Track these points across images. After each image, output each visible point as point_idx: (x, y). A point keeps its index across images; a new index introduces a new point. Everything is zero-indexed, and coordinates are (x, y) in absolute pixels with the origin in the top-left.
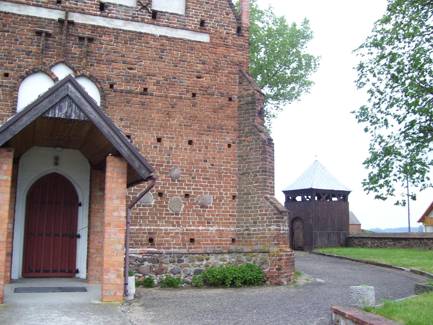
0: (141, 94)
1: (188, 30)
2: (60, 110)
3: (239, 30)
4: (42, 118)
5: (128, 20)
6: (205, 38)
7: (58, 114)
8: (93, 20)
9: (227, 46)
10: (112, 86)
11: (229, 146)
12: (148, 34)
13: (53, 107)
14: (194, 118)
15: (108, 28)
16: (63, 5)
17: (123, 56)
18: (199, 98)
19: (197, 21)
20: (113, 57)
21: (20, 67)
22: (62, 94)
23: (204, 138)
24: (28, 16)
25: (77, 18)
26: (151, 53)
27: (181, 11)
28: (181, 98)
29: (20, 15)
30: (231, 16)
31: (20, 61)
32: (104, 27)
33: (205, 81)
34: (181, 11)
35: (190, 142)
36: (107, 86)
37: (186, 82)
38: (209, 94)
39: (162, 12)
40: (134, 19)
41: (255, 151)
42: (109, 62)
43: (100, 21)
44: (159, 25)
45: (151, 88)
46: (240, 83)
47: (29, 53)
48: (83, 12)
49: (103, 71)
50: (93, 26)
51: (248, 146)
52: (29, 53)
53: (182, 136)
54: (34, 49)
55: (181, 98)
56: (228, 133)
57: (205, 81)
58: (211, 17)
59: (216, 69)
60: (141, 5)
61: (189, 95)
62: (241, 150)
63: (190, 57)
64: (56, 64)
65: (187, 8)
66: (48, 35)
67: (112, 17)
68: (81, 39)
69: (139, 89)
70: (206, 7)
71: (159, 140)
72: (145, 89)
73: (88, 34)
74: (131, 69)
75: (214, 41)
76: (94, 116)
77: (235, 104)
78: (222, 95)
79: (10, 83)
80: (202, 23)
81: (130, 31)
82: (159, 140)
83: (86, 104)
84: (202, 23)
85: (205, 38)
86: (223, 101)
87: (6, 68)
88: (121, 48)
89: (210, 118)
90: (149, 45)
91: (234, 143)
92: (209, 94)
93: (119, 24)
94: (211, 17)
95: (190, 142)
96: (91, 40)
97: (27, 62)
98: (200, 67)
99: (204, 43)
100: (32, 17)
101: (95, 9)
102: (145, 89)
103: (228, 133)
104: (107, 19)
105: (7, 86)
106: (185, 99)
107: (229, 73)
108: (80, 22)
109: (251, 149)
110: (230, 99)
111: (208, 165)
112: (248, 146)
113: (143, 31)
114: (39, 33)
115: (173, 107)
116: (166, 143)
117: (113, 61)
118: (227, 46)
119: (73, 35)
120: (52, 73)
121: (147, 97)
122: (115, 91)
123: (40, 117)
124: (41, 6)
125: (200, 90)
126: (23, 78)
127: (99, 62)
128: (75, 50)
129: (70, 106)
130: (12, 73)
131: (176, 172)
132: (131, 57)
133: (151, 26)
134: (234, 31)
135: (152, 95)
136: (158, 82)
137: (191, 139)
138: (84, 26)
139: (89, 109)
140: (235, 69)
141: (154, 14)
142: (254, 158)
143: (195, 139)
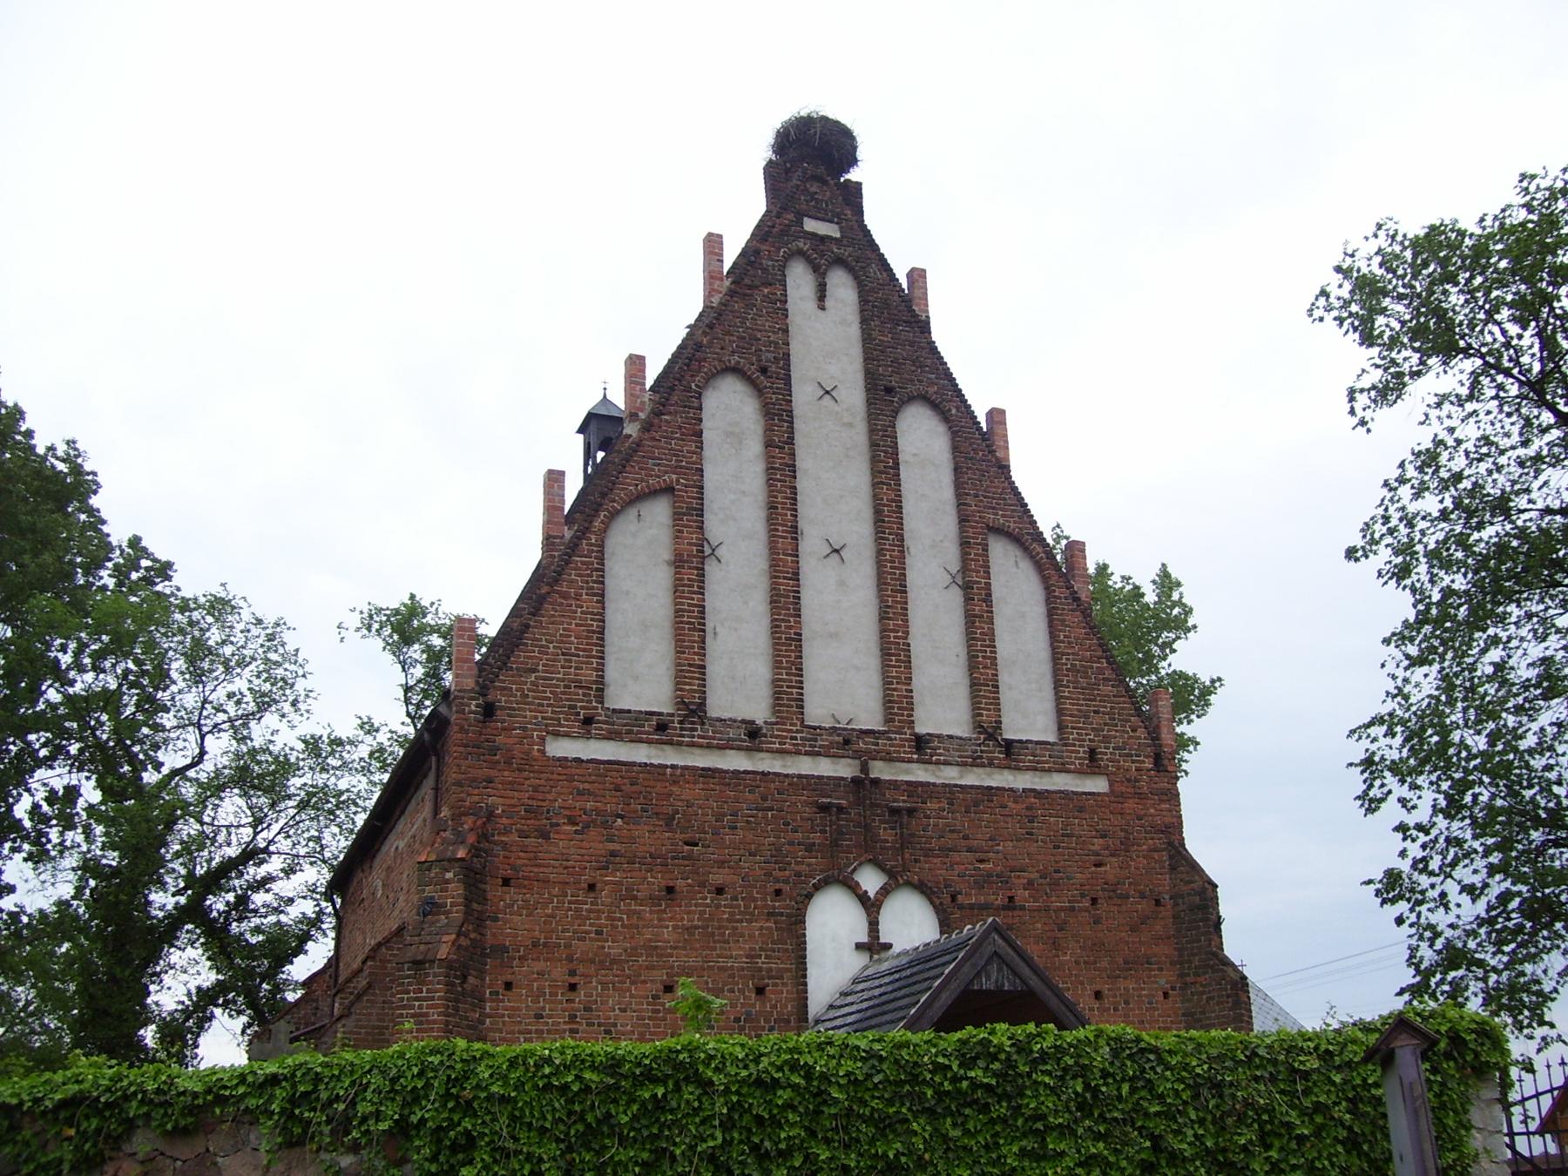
0: (1005, 908)
1: (1068, 771)
2: (988, 978)
5: (964, 764)
6: (1099, 785)
7: (986, 984)
8: (908, 772)
9: (1141, 796)
10: (953, 898)
11: (1166, 995)
12: (1003, 789)
13: (978, 974)
15: (934, 784)
16: (855, 747)
17: (966, 837)
18: (1103, 905)
19: (1082, 752)
21: (798, 874)
22: (988, 950)
23: (1121, 984)
24: (800, 776)
25: (880, 770)
27: (1051, 737)
28: (1073, 909)
29: (787, 776)
30: (1141, 732)
31: (797, 863)
32: (928, 784)
33: (1110, 870)
34: (1051, 737)
35: (1098, 995)
36: (947, 899)
38: (1120, 897)
39: (1020, 741)
40: (975, 762)
41: (1218, 1003)
42: (946, 851)
43: (920, 774)
44: (1018, 769)
45: (1022, 895)
46: (1173, 868)
47: (810, 848)
48: (889, 758)
50: (909, 783)
51: (1203, 993)
52: (810, 848)
53: (1082, 983)
54: (816, 838)
55: (1073, 909)
56: (1161, 969)
57: (1110, 870)
58: (1107, 740)
60: (985, 731)
62: (1189, 1001)
64: (860, 864)
65: (1061, 727)
66: (840, 809)
67: (938, 763)
68: (895, 812)
69: (1000, 901)
70: (1096, 720)
72: (1011, 899)
73: (901, 802)
74: (981, 861)
75: (1120, 788)
76: (1034, 982)
77: (1167, 912)
78: (1143, 896)
79: (787, 907)
80: (1092, 753)
81: (972, 787)
83: (1022, 964)
85: (1099, 785)
86: (1144, 906)
87: (777, 880)
89: (1127, 943)
90: (1006, 811)
91: (1173, 989)
92: (1120, 897)
93: (950, 775)
96: (911, 812)
97: (809, 865)
99: (1099, 794)
100: (807, 777)
101: (907, 751)
102: (1011, 899)
103: (1161, 969)
104: (930, 767)
105: (781, 914)
106: (1081, 910)
107: (1150, 850)
108: (886, 777)
109: (1208, 999)
112: (1203, 993)
113: (994, 784)
114: (824, 808)
115: (1061, 930)
117: (950, 850)
118: (1141, 796)
119: (878, 806)
120: (857, 884)
121: (1017, 913)
122: (961, 907)
123: (963, 992)
124: (818, 754)
125: (1103, 890)
126: (809, 896)
127: (928, 853)
128: (886, 834)
129: (1000, 970)
130: (786, 888)
133: (1006, 772)
135: (1023, 908)
136: (1030, 883)
137: (1098, 988)
138: (894, 784)
139: (1026, 972)
141: (1009, 745)
142: (1218, 1017)
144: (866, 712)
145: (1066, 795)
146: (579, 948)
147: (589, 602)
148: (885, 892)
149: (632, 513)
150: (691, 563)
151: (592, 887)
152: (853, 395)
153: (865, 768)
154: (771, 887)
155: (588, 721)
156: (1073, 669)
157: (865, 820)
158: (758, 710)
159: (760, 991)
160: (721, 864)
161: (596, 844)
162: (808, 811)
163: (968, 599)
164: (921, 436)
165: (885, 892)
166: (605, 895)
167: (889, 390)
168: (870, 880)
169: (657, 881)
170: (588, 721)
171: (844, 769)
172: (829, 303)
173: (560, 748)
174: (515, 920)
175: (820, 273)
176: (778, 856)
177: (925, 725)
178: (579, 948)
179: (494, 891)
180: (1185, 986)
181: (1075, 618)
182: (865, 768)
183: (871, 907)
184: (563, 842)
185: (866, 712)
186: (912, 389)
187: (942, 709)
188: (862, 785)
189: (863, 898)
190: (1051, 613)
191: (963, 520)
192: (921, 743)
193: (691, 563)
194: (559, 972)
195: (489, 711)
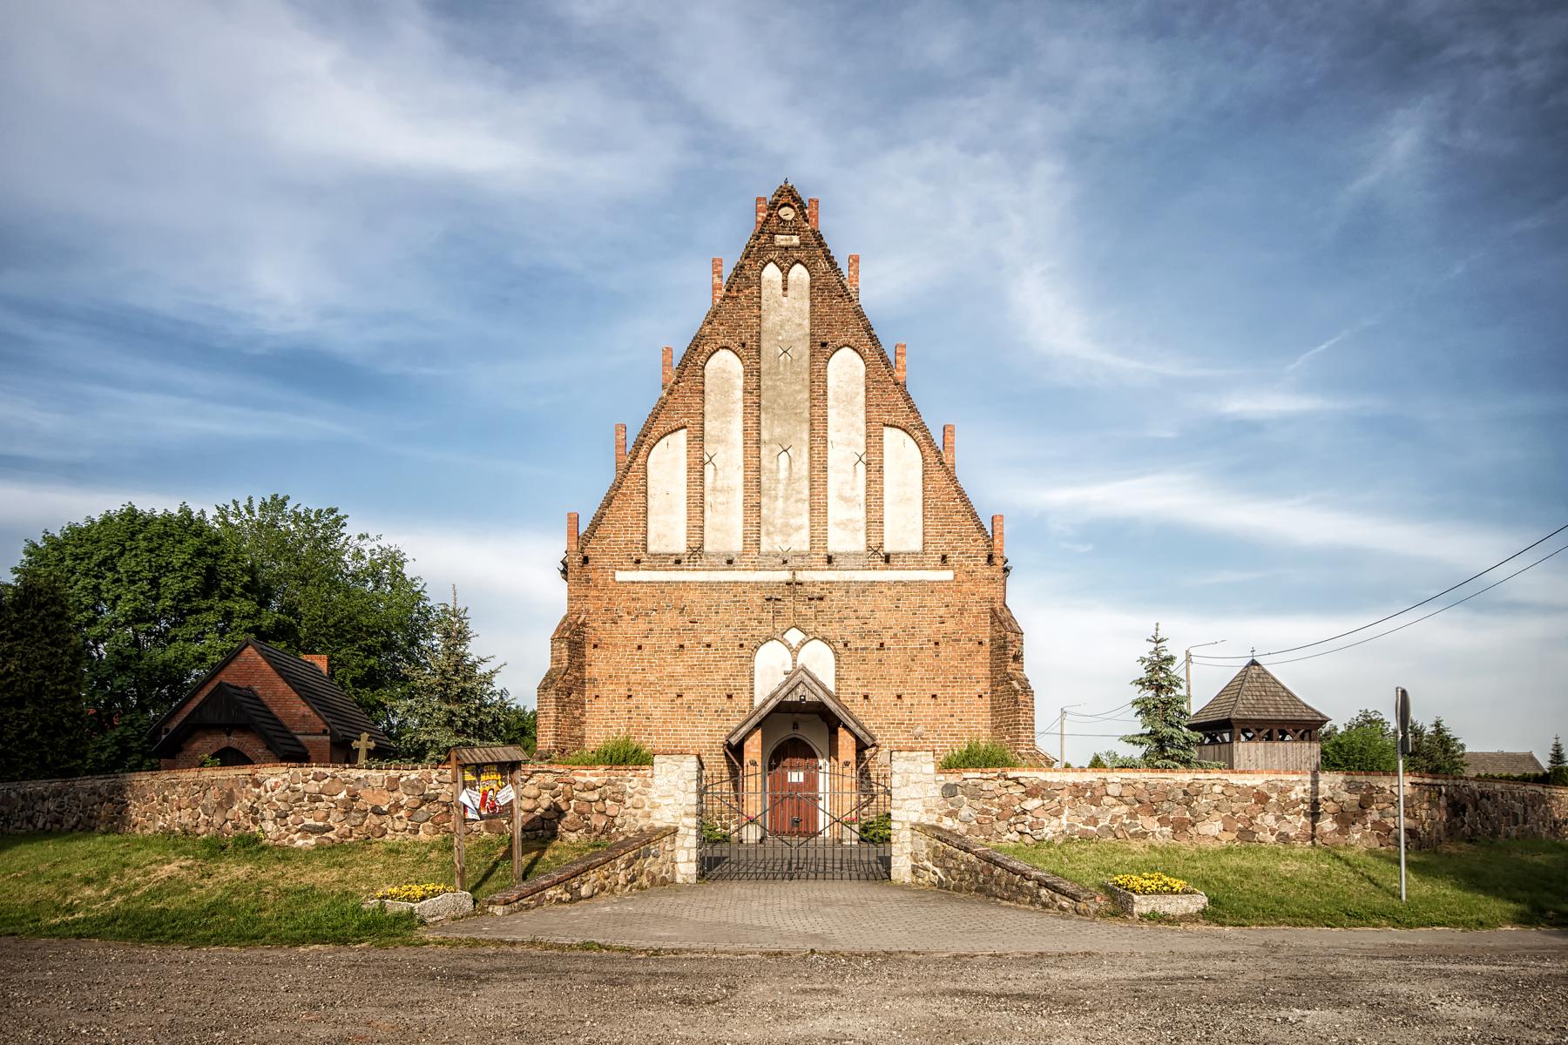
3: (990, 558)
18: (942, 646)
19: (938, 557)
20: (845, 613)
23: (950, 691)
25: (801, 576)
26: (887, 604)
30: (981, 543)
33: (950, 626)
35: (934, 696)
36: (840, 646)
42: (841, 620)
45: (888, 642)
49: (833, 630)
58: (954, 549)
59: (962, 611)
61: (932, 645)
63: (932, 602)
69: (876, 645)
70: (949, 537)
73: (817, 592)
77: (987, 647)
80: (944, 558)
82: (899, 697)
84: (944, 558)
85: (947, 575)
94: (954, 549)
95: (934, 696)
98: (942, 611)
101: (822, 563)
111: (953, 720)
116: (907, 700)
131: (919, 730)
134: (983, 561)
138: (813, 584)
140: (986, 606)
141: (887, 559)
143: (938, 693)
145: (922, 583)
146: (633, 678)
147: (639, 499)
148: (803, 644)
149: (663, 441)
150: (698, 468)
151: (640, 647)
152: (804, 348)
154: (737, 643)
155: (638, 562)
156: (936, 507)
157: (791, 603)
158: (736, 545)
159: (730, 697)
160: (709, 632)
161: (642, 625)
163: (868, 471)
164: (846, 368)
165: (803, 644)
166: (646, 651)
167: (824, 345)
168: (794, 636)
169: (675, 642)
170: (638, 562)
171: (785, 576)
172: (790, 293)
173: (621, 576)
174: (597, 665)
175: (786, 272)
176: (743, 629)
177: (833, 547)
178: (633, 678)
179: (589, 650)
180: (993, 692)
181: (939, 476)
183: (794, 652)
184: (626, 625)
186: (838, 343)
187: (845, 537)
189: (789, 647)
190: (925, 472)
191: (868, 422)
192: (830, 560)
194: (623, 690)
195: (586, 560)
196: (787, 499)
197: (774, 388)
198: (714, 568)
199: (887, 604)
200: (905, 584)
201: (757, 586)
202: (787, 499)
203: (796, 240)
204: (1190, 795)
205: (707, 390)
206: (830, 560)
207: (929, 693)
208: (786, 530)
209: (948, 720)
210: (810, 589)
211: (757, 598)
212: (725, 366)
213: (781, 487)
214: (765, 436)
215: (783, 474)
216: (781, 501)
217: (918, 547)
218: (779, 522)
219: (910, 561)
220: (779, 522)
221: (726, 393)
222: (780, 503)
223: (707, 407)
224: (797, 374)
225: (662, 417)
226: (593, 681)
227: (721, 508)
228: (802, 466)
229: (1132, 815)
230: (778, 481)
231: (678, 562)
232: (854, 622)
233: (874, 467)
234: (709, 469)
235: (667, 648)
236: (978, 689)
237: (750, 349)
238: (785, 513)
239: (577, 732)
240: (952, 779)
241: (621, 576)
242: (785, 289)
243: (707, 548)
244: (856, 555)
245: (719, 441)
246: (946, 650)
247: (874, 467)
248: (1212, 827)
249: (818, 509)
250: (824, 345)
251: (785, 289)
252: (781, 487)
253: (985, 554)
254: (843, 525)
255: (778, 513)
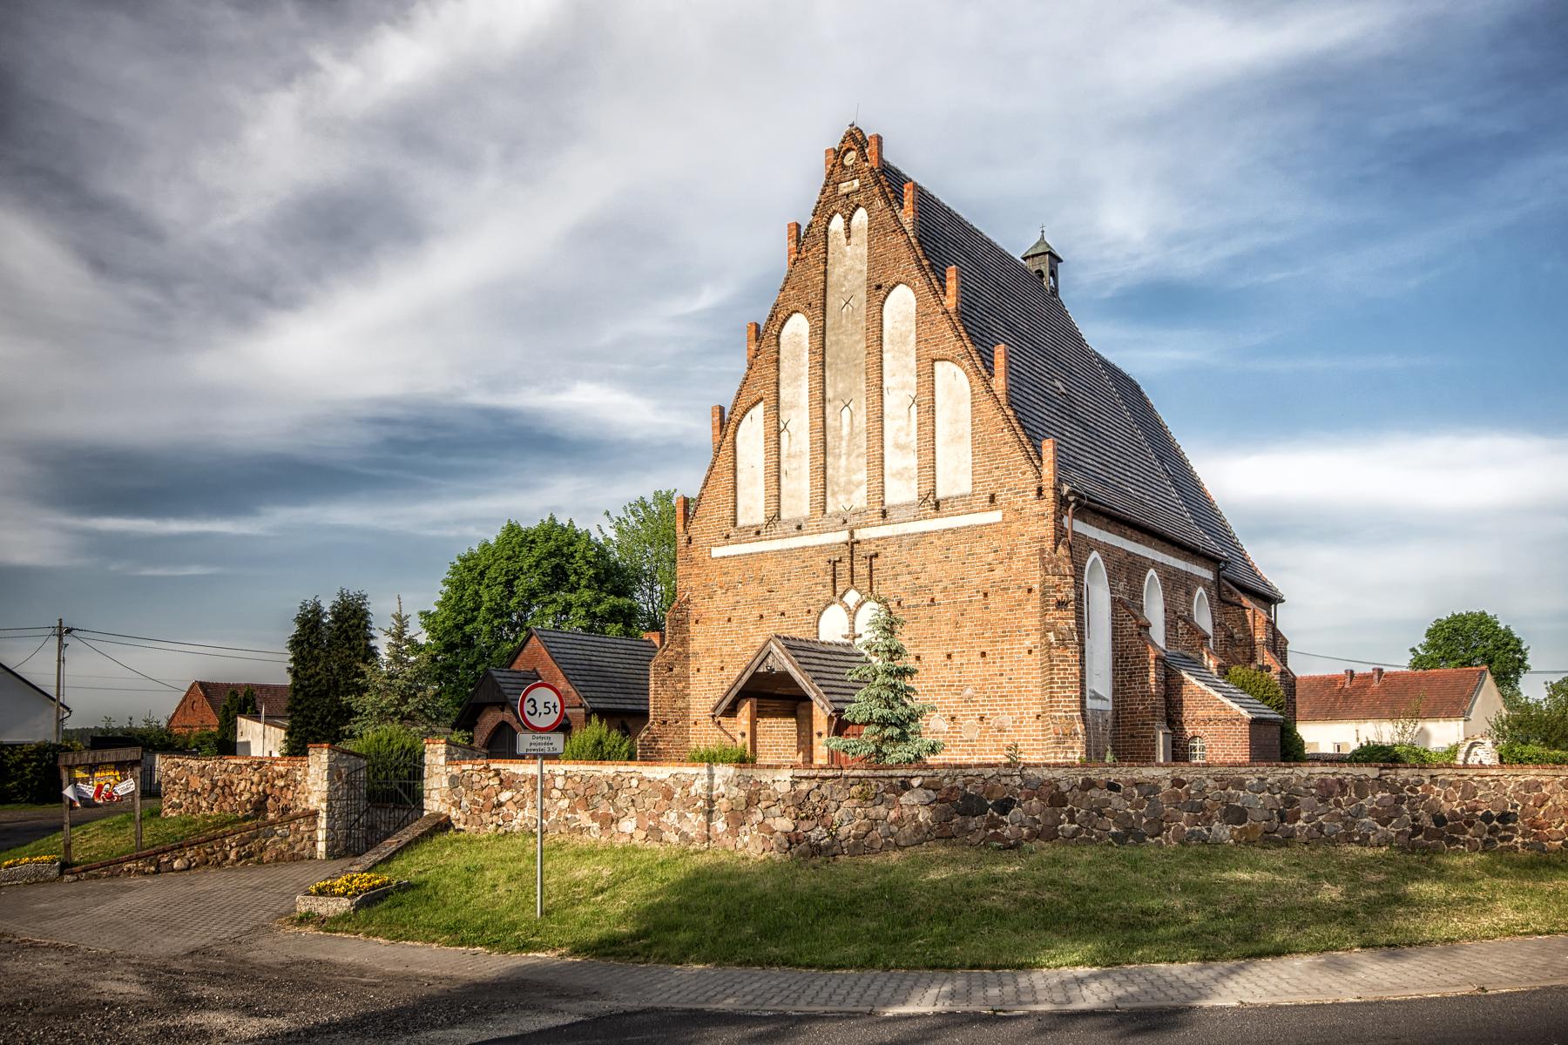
4: (755, 675)
14: (984, 624)
19: (985, 498)
20: (899, 569)
25: (859, 535)
26: (938, 555)
30: (1030, 475)
33: (999, 573)
35: (983, 654)
37: (976, 581)
45: (938, 597)
48: (867, 525)
57: (999, 573)
58: (1002, 485)
69: (927, 601)
70: (997, 473)
71: (949, 656)
73: (872, 549)
80: (992, 498)
82: (949, 656)
84: (992, 498)
85: (995, 516)
88: (905, 556)
95: (983, 654)
101: (877, 518)
110: (1030, 591)
111: (1004, 680)
116: (956, 659)
131: (969, 692)
132: (916, 567)
134: (1032, 495)
138: (869, 541)
144: (859, 499)
148: (860, 605)
150: (776, 433)
153: (852, 534)
162: (823, 565)
166: (734, 621)
167: (879, 287)
169: (756, 613)
171: (844, 536)
172: (852, 240)
173: (717, 552)
179: (692, 627)
182: (852, 534)
183: (852, 614)
185: (859, 499)
188: (852, 544)
189: (848, 609)
193: (776, 433)
194: (717, 663)
195: (690, 540)
196: (849, 455)
197: (837, 342)
198: (786, 536)
199: (938, 555)
200: (954, 531)
201: (821, 549)
202: (849, 455)
203: (856, 183)
204: (614, 789)
205: (782, 357)
206: (884, 514)
207: (978, 650)
208: (848, 490)
209: (998, 680)
210: (866, 547)
211: (821, 563)
212: (798, 328)
213: (844, 444)
214: (830, 394)
215: (845, 431)
216: (844, 458)
217: (968, 489)
218: (842, 480)
219: (959, 505)
220: (842, 480)
221: (797, 357)
222: (843, 461)
223: (782, 375)
224: (856, 323)
225: (744, 393)
226: (696, 654)
227: (794, 474)
228: (861, 420)
229: (572, 810)
230: (841, 438)
231: (758, 533)
232: (909, 577)
233: (927, 407)
234: (784, 435)
235: (750, 618)
236: (1028, 643)
237: (819, 310)
238: (848, 470)
239: (680, 704)
240: (455, 770)
241: (717, 552)
242: (848, 237)
243: (784, 516)
244: (907, 505)
245: (791, 407)
246: (995, 601)
247: (927, 407)
248: (628, 825)
249: (878, 462)
250: (879, 287)
251: (848, 237)
252: (844, 444)
253: (1034, 487)
254: (899, 474)
255: (842, 471)
